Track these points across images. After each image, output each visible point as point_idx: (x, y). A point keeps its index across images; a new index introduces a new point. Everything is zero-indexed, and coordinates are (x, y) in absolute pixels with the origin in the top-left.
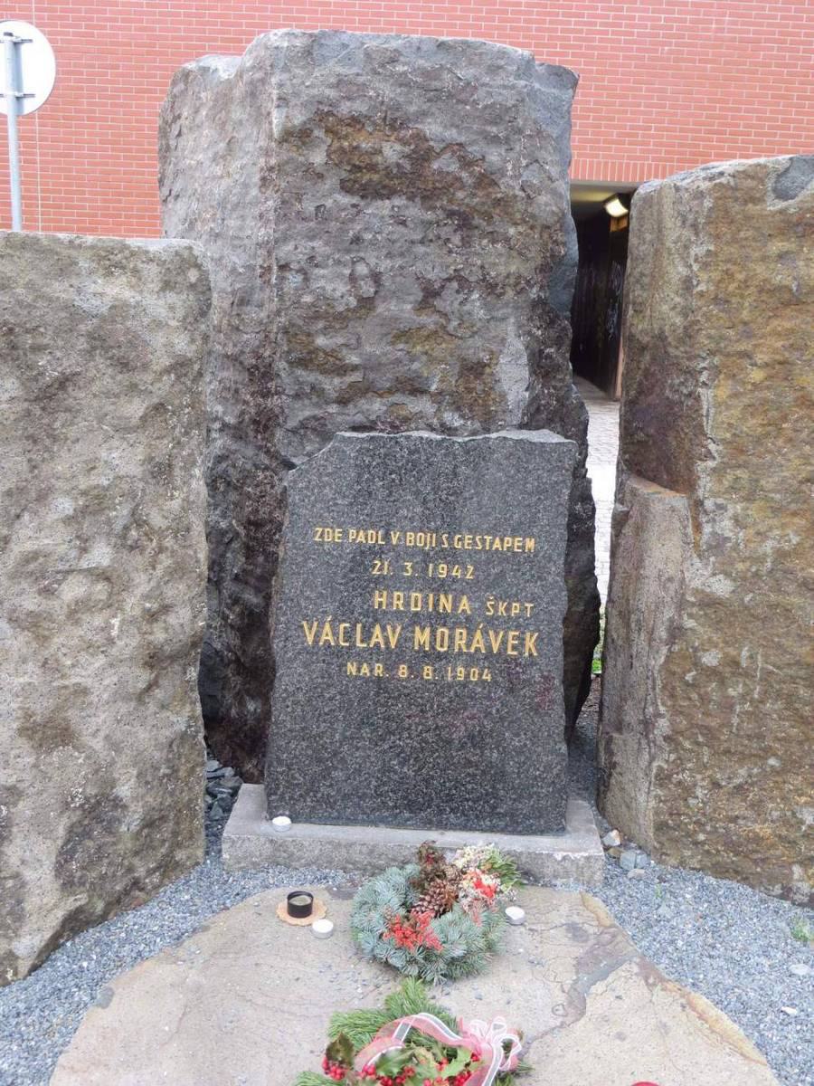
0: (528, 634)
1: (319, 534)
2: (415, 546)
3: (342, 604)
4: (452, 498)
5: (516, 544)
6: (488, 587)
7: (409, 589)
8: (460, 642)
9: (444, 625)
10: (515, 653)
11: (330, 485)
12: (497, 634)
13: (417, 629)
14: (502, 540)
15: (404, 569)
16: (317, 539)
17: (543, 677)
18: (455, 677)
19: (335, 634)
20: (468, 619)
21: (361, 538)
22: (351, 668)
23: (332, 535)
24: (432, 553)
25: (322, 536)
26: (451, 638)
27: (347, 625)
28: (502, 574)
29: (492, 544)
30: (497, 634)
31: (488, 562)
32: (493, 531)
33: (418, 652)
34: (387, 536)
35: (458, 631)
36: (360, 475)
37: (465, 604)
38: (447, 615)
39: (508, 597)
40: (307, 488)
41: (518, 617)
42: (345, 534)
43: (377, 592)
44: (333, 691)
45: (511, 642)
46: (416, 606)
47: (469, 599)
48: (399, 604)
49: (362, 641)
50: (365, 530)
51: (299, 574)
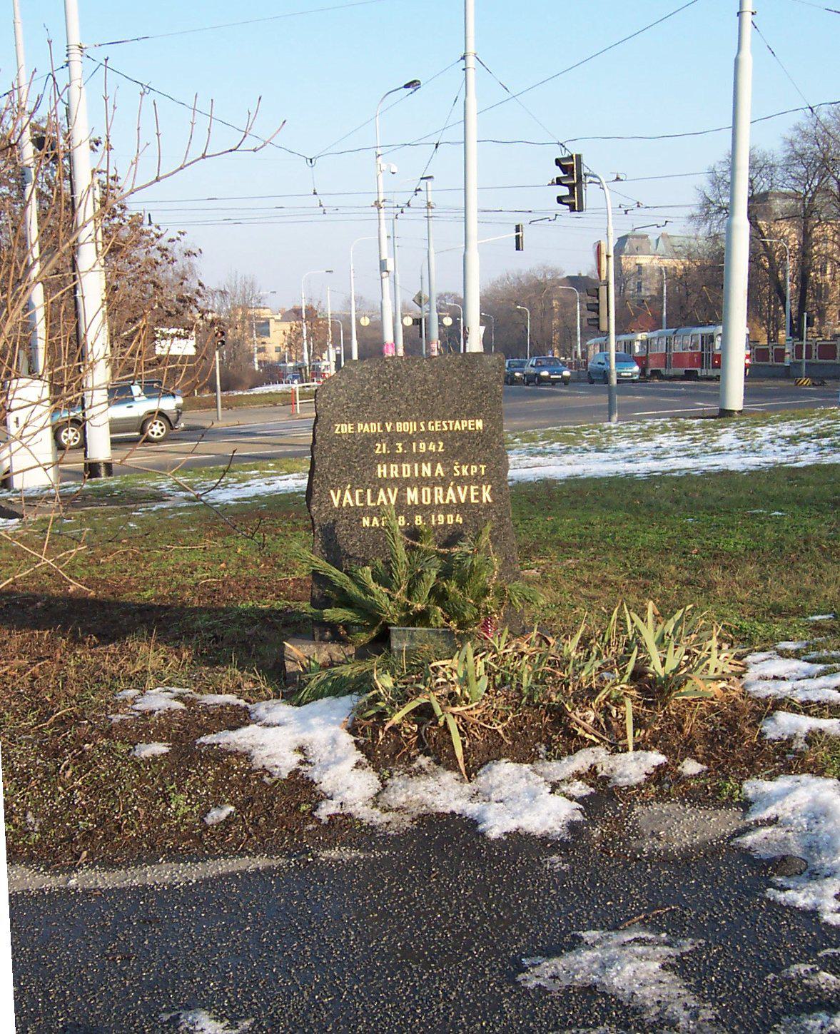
0: (484, 487)
1: (338, 429)
2: (403, 432)
3: (357, 476)
4: (425, 397)
5: (470, 425)
6: (454, 456)
7: (402, 462)
8: (439, 498)
9: (427, 486)
10: (477, 501)
11: (343, 394)
12: (463, 488)
13: (409, 490)
14: (460, 423)
15: (396, 448)
16: (337, 432)
17: (497, 517)
18: (437, 522)
19: (353, 497)
20: (442, 479)
21: (366, 428)
22: (366, 522)
23: (345, 429)
24: (414, 436)
25: (340, 430)
26: (433, 494)
27: (361, 491)
28: (463, 447)
29: (453, 426)
30: (463, 488)
31: (453, 438)
32: (453, 418)
33: (411, 506)
34: (383, 427)
35: (436, 489)
36: (363, 386)
37: (439, 470)
38: (428, 478)
39: (468, 461)
40: (328, 398)
41: (476, 475)
42: (356, 426)
43: (379, 466)
44: (354, 539)
45: (473, 494)
46: (406, 473)
47: (442, 466)
48: (394, 473)
49: (372, 501)
50: (369, 424)
51: (326, 457)
